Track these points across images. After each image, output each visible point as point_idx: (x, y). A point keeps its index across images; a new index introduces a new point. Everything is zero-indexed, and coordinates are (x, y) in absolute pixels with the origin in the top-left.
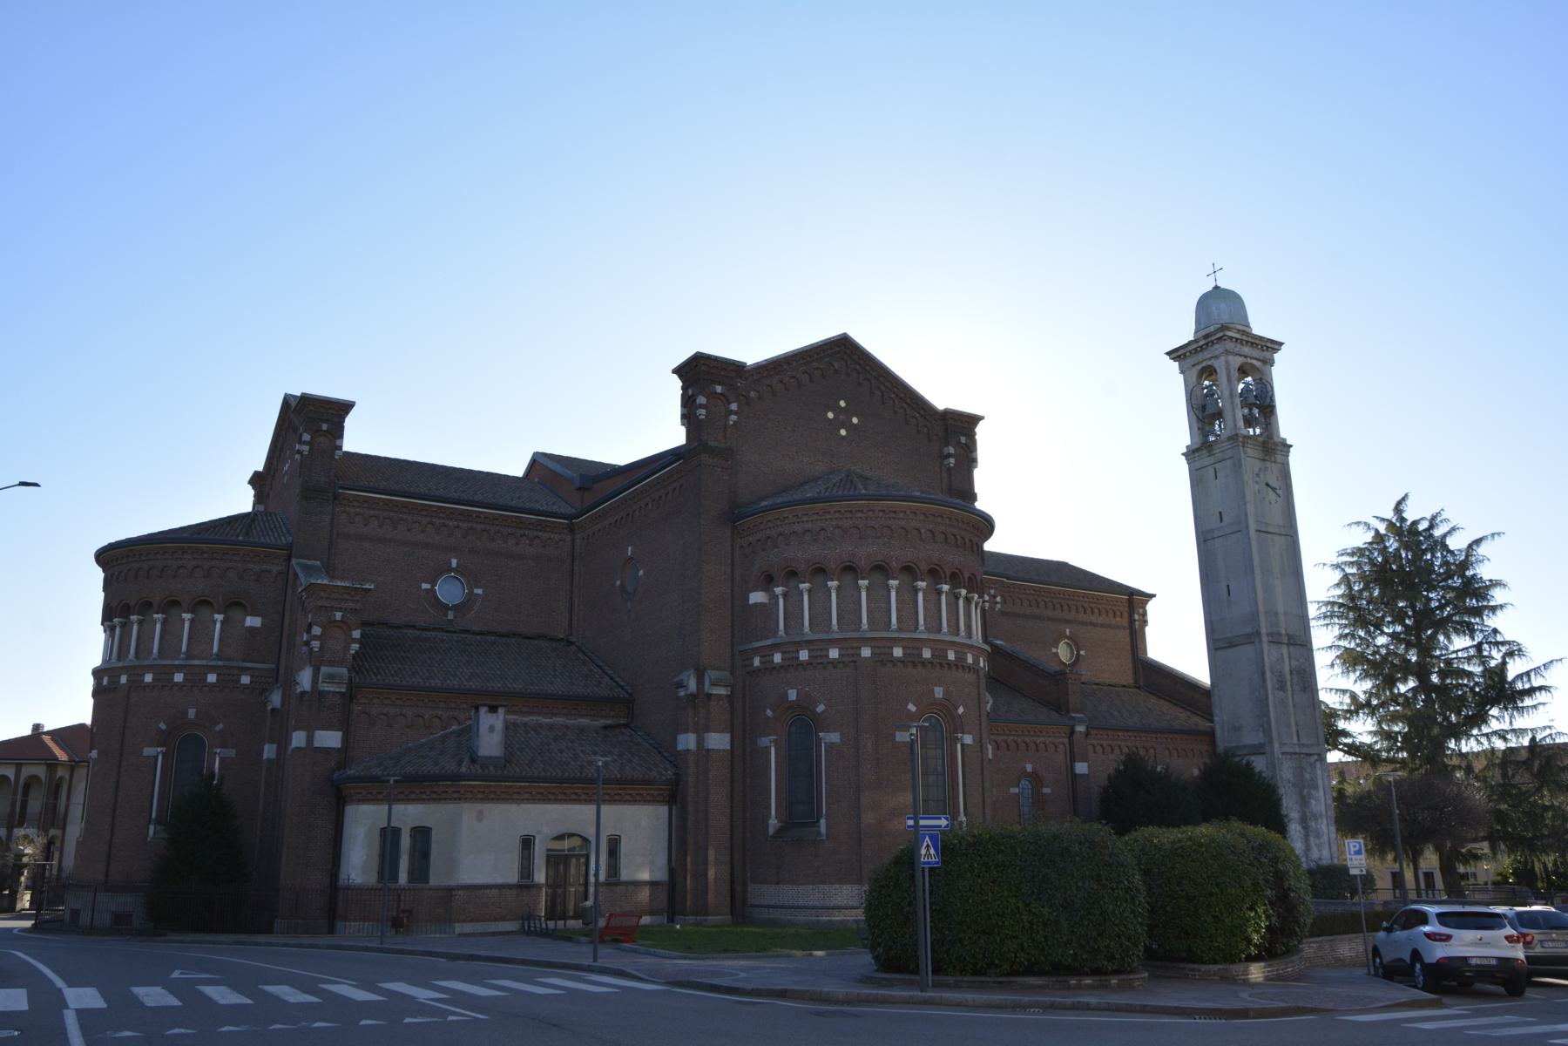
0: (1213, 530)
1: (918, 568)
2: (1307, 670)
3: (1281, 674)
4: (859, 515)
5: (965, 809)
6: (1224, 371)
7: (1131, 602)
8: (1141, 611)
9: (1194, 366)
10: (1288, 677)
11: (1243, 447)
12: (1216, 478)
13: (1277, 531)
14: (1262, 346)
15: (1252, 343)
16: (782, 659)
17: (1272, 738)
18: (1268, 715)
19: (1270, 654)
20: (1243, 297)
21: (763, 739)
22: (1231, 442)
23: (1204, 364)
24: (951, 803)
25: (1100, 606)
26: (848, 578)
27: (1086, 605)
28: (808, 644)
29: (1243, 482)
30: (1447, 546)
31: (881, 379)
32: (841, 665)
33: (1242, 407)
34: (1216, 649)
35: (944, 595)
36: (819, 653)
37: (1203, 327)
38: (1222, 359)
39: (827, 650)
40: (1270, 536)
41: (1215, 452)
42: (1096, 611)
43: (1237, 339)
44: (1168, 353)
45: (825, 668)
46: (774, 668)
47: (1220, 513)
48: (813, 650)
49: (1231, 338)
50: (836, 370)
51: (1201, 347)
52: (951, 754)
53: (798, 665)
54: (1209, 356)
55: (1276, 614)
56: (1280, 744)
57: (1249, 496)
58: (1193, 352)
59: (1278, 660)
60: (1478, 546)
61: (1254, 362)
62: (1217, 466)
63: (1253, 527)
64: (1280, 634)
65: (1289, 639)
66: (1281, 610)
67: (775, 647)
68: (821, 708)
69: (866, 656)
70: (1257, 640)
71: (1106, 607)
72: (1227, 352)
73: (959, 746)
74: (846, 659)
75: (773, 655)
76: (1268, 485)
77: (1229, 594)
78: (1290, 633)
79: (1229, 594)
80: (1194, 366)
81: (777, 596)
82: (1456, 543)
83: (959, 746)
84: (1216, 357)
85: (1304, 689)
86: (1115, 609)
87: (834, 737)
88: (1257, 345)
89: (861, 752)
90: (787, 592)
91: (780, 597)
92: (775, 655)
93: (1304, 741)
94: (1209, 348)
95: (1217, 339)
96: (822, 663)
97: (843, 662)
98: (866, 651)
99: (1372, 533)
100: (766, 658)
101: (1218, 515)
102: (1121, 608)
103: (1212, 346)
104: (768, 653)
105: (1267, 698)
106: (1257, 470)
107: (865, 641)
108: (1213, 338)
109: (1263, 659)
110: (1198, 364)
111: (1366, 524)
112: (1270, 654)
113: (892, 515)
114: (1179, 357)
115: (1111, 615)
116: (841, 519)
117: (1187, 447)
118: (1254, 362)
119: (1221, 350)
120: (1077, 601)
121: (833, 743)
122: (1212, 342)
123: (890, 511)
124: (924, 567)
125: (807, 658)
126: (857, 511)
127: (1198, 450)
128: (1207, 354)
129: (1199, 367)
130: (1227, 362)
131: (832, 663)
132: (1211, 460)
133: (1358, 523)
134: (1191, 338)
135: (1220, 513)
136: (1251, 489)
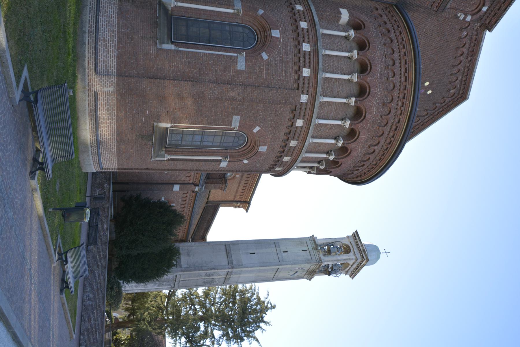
0: (280, 248)
1: (352, 142)
2: (213, 284)
3: (212, 275)
4: (400, 104)
5: (173, 160)
6: (349, 258)
7: (246, 202)
8: (241, 206)
9: (351, 242)
10: (211, 277)
11: (316, 264)
12: (302, 251)
13: (276, 275)
14: (354, 272)
15: (357, 269)
16: (303, 28)
17: (184, 272)
18: (195, 270)
19: (223, 273)
20: (375, 264)
21: (240, 4)
22: (319, 260)
23: (351, 248)
24: (178, 150)
25: (246, 190)
26: (355, 90)
27: (248, 184)
28: (316, 52)
29: (300, 264)
30: (256, 330)
31: (431, 117)
32: (296, 77)
33: (332, 264)
34: (226, 245)
35: (327, 156)
36: (307, 60)
37: (367, 248)
38: (354, 257)
39: (309, 67)
40: (275, 272)
41: (314, 251)
42: (245, 188)
43: (361, 264)
44: (356, 231)
45: (296, 63)
46: (296, 21)
47: (287, 252)
48: (309, 55)
49: (362, 262)
50: (450, 90)
51: (359, 247)
52: (215, 152)
53: (299, 42)
54: (355, 250)
55: (240, 274)
56: (181, 275)
57: (294, 266)
58: (357, 243)
59: (219, 274)
60: (256, 341)
61: (348, 268)
62: (308, 251)
63: (280, 267)
64: (230, 275)
65: (228, 278)
66: (241, 275)
67: (312, 24)
68: (265, 56)
69: (301, 98)
70: (230, 267)
71: (246, 192)
72: (357, 260)
73: (220, 158)
74: (301, 81)
75: (305, 21)
76: (297, 272)
77: (251, 254)
78: (230, 278)
79: (251, 254)
80: (351, 242)
81: (348, 32)
82: (258, 333)
83: (220, 158)
84: (355, 254)
85: (204, 282)
86: (244, 196)
87: (241, 65)
88: (356, 270)
89: (229, 86)
90: (348, 40)
91: (347, 33)
92: (305, 23)
93: (181, 282)
94: (358, 251)
95: (363, 256)
96: (299, 61)
97: (299, 79)
98: (305, 99)
99: (264, 300)
100: (303, 16)
101: (286, 251)
102: (243, 198)
103: (359, 252)
104: (307, 17)
105: (203, 270)
106: (304, 269)
107: (313, 99)
108: (363, 254)
109: (221, 269)
110: (351, 245)
111: (268, 297)
112: (223, 273)
113: (394, 127)
114: (355, 236)
115: (242, 194)
116: (399, 90)
117: (316, 237)
118: (348, 268)
119: (358, 257)
120: (251, 181)
121: (237, 63)
122: (361, 253)
123: (397, 127)
124: (352, 146)
125: (304, 50)
126: (403, 103)
127: (315, 243)
128: (356, 250)
129: (350, 245)
130: (352, 259)
131: (299, 70)
132: (310, 249)
133: (268, 294)
134: (363, 242)
135: (287, 252)
136: (297, 267)
